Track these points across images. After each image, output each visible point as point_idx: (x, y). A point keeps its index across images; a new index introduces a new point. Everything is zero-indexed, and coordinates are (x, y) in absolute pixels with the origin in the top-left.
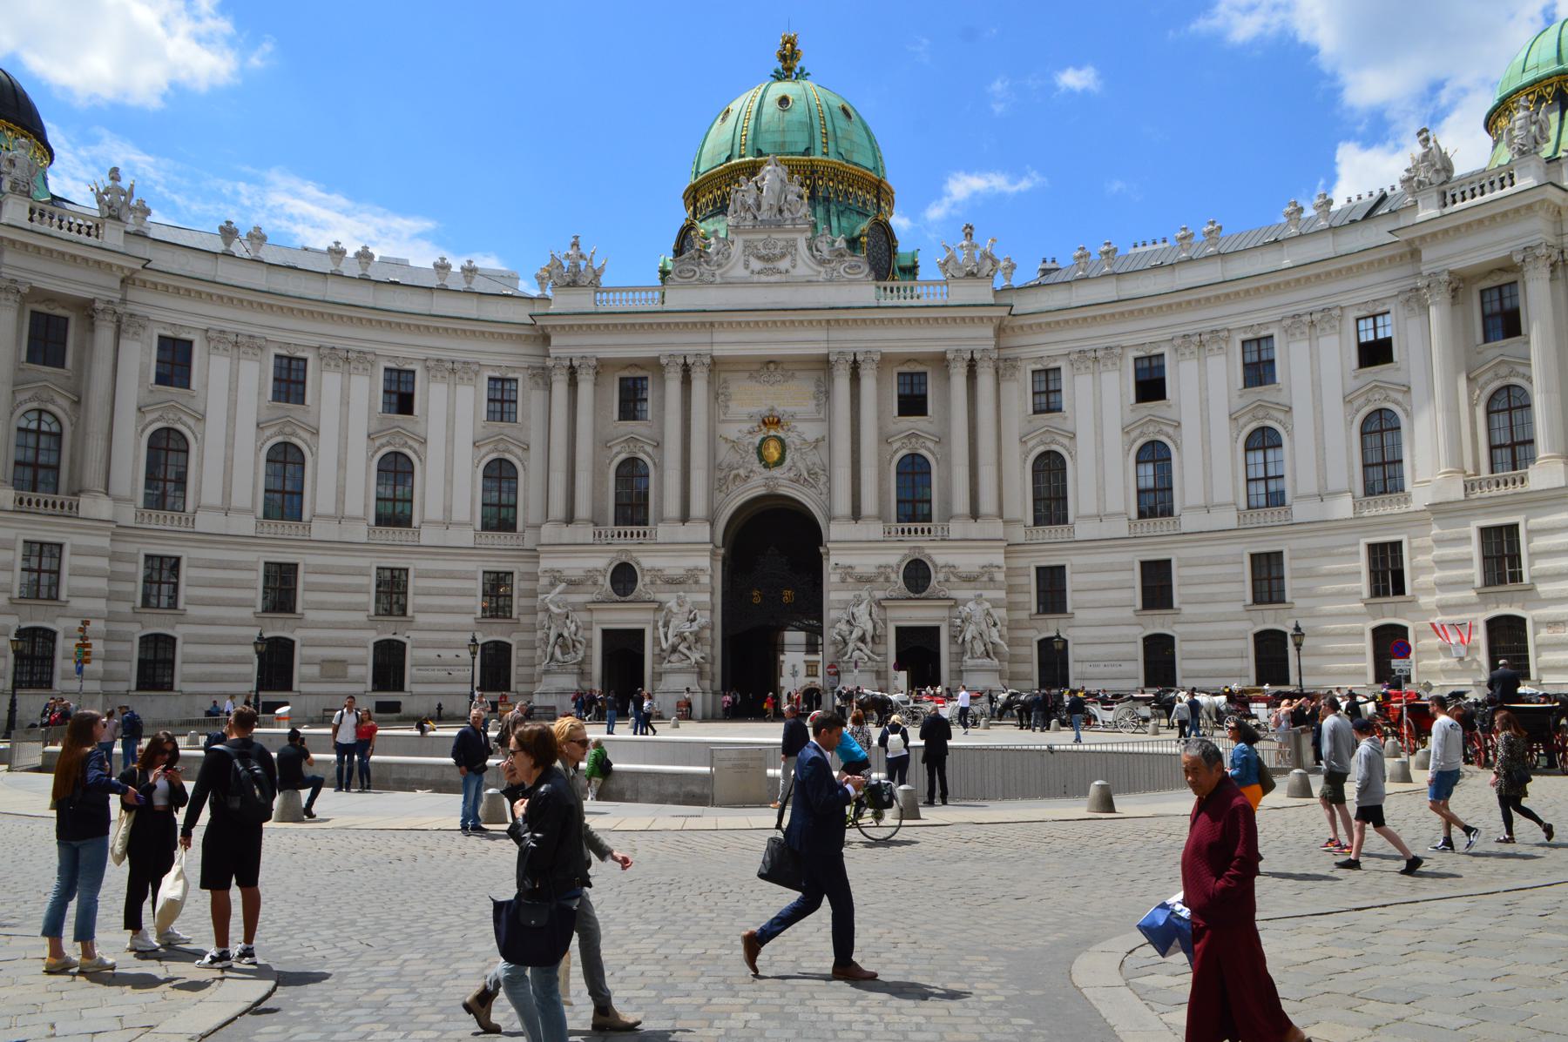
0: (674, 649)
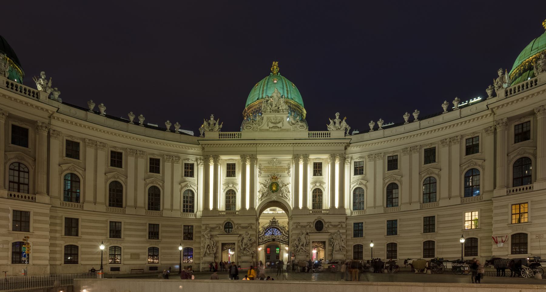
0: (244, 249)
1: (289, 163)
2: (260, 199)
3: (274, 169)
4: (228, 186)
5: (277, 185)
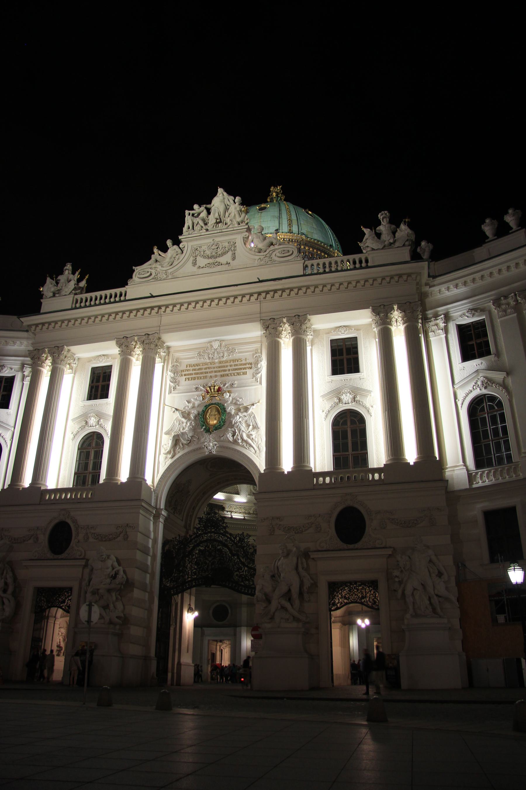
1: (257, 350)
2: (169, 452)
3: (216, 369)
4: (87, 423)
5: (221, 409)
